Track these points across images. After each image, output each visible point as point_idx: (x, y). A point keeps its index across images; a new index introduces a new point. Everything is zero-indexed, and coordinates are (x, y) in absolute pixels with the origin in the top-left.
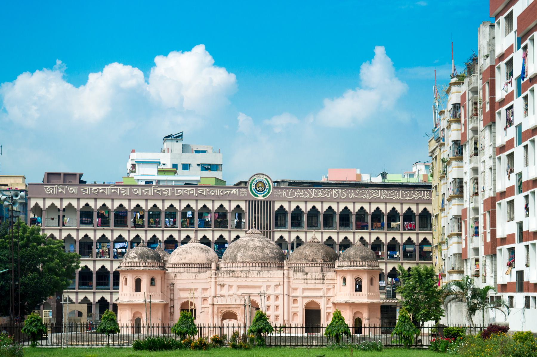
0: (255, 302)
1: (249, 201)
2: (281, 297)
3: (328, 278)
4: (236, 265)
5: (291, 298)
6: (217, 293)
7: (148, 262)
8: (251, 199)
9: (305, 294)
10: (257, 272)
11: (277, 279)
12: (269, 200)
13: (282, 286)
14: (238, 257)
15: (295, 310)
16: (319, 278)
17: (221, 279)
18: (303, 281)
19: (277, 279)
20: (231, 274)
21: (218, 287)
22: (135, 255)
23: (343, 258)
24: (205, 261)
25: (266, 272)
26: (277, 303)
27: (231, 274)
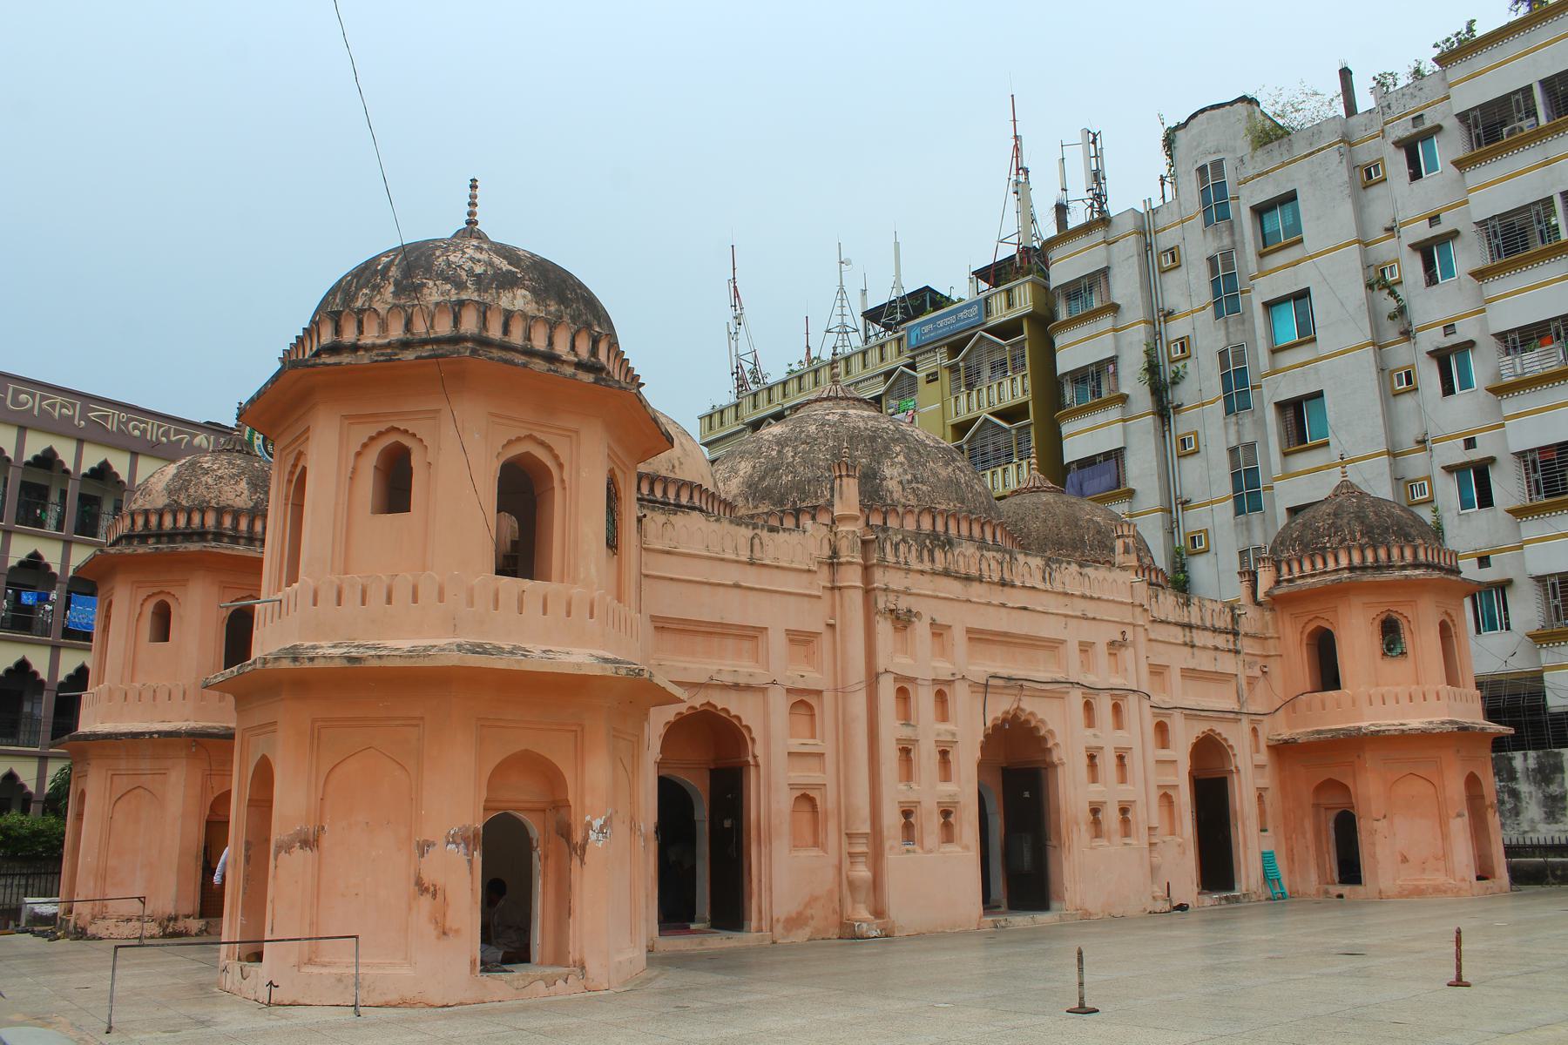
0: (1036, 728)
2: (1131, 705)
3: (1248, 630)
6: (881, 670)
9: (1190, 702)
11: (1115, 613)
14: (892, 485)
15: (1169, 780)
16: (1220, 624)
17: (896, 580)
18: (1178, 635)
19: (1115, 613)
20: (938, 554)
21: (884, 627)
22: (504, 265)
23: (1368, 532)
25: (1074, 568)
27: (938, 554)
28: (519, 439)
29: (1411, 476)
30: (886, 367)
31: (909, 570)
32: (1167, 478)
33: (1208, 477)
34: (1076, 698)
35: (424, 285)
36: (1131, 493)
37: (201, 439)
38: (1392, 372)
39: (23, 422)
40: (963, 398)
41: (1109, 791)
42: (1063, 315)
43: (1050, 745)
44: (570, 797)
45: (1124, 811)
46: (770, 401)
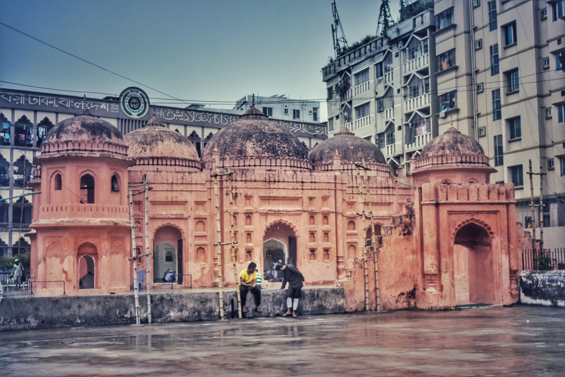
0: (289, 226)
1: (122, 120)
2: (332, 217)
4: (247, 164)
5: (345, 218)
6: (225, 211)
7: (109, 144)
8: (124, 118)
10: (291, 172)
12: (145, 120)
13: (332, 199)
24: (187, 157)
26: (326, 227)
28: (85, 171)
29: (547, 106)
30: (383, 49)
31: (236, 181)
32: (472, 104)
33: (485, 103)
34: (306, 216)
35: (61, 137)
36: (457, 111)
37: (103, 106)
38: (544, 59)
39: (36, 108)
40: (407, 64)
41: (320, 244)
42: (441, 28)
43: (295, 230)
44: (98, 252)
45: (326, 250)
46: (345, 63)
